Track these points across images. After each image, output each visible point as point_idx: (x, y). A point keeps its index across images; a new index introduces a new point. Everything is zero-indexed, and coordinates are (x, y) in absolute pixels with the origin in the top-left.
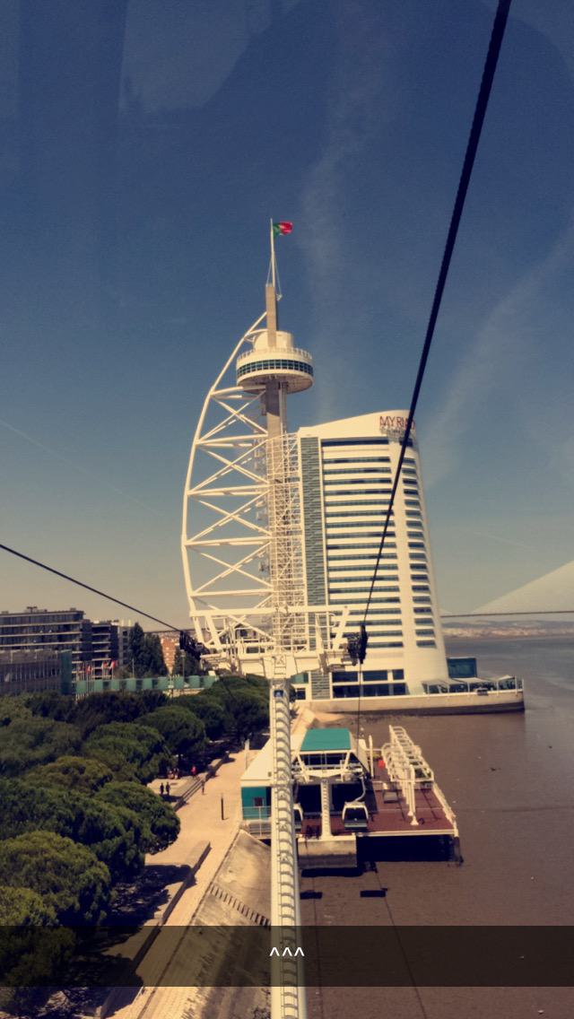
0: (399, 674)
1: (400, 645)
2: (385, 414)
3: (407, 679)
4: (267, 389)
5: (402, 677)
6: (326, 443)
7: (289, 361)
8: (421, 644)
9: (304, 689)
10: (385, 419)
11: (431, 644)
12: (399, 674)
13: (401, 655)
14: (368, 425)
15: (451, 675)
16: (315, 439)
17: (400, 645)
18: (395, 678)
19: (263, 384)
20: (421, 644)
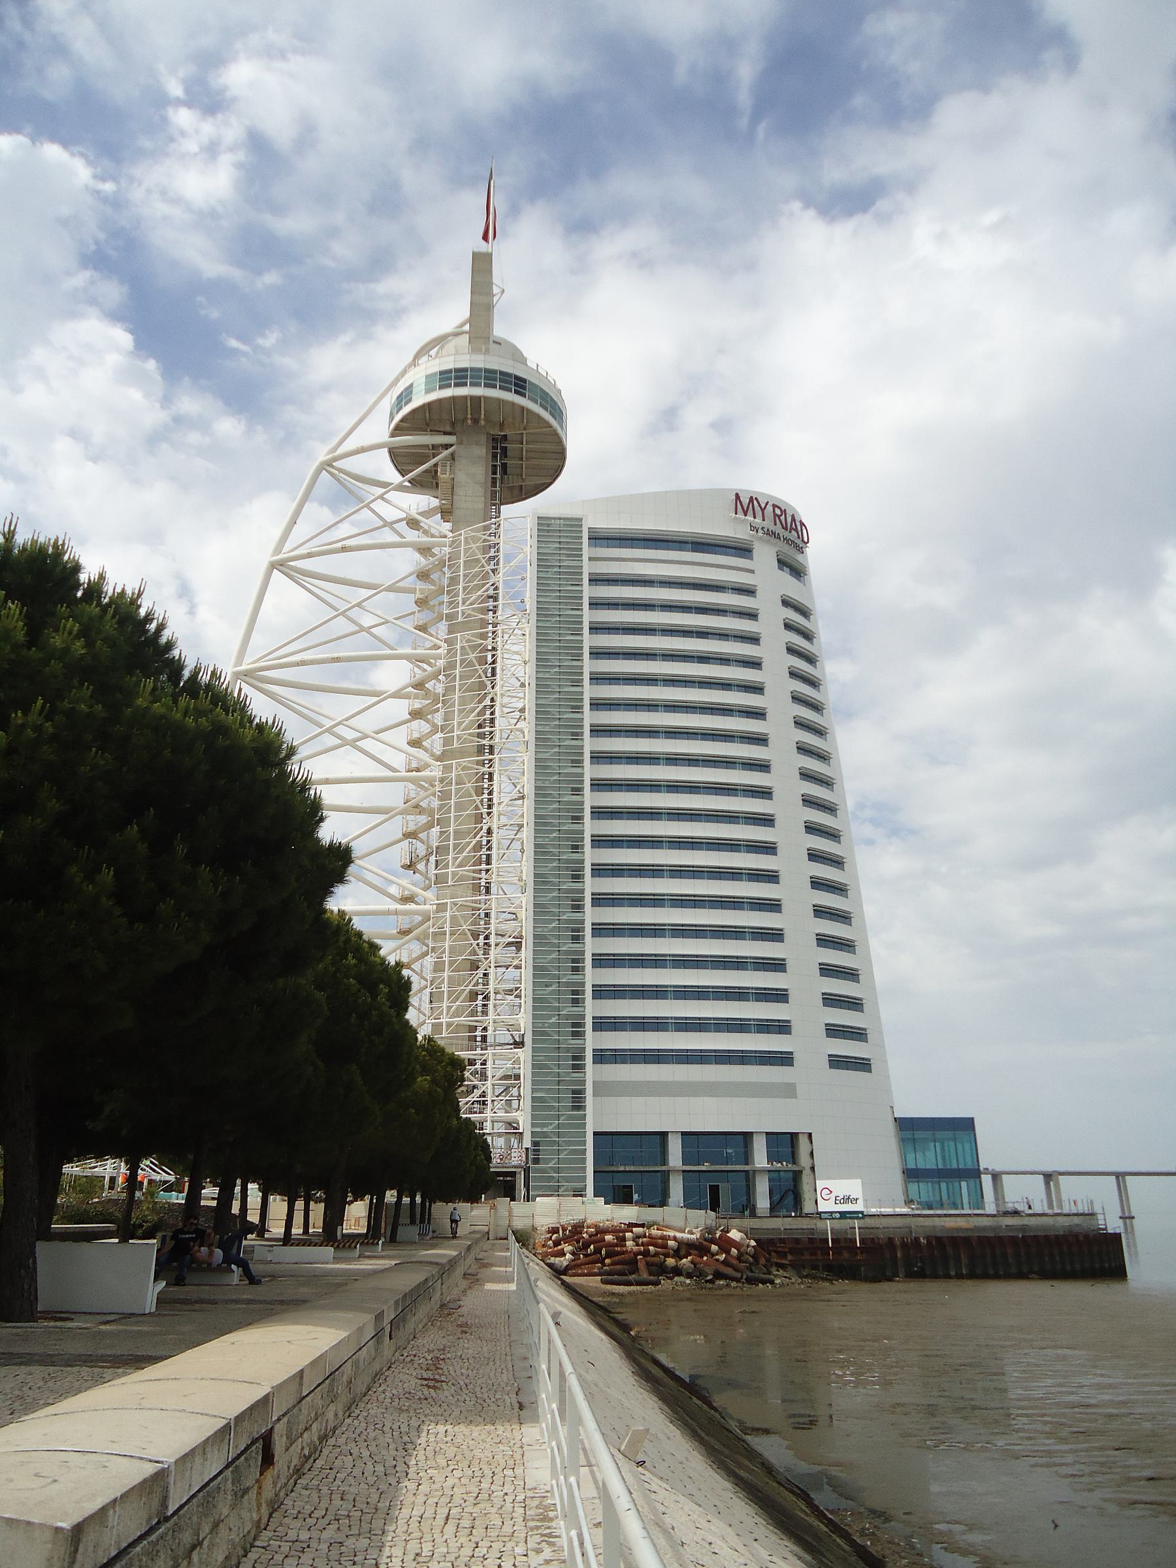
1: (784, 1059)
4: (460, 442)
6: (597, 538)
10: (745, 501)
16: (575, 524)
17: (784, 1059)
19: (445, 433)
20: (837, 1062)
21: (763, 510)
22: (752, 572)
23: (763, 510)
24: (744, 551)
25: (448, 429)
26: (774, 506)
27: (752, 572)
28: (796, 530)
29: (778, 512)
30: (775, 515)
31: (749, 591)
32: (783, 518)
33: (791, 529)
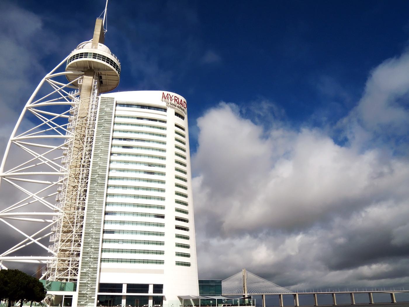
0: (158, 288)
1: (161, 262)
2: (166, 93)
3: (165, 292)
5: (162, 293)
7: (103, 56)
8: (178, 263)
9: (72, 296)
10: (166, 95)
11: (188, 265)
12: (158, 288)
13: (161, 272)
14: (154, 97)
15: (200, 293)
17: (161, 262)
18: (154, 292)
19: (82, 71)
20: (178, 263)
21: (171, 98)
22: (166, 116)
23: (171, 98)
24: (165, 110)
25: (83, 70)
26: (175, 97)
27: (166, 116)
28: (182, 104)
29: (176, 98)
30: (175, 99)
31: (165, 122)
32: (177, 100)
33: (180, 103)
